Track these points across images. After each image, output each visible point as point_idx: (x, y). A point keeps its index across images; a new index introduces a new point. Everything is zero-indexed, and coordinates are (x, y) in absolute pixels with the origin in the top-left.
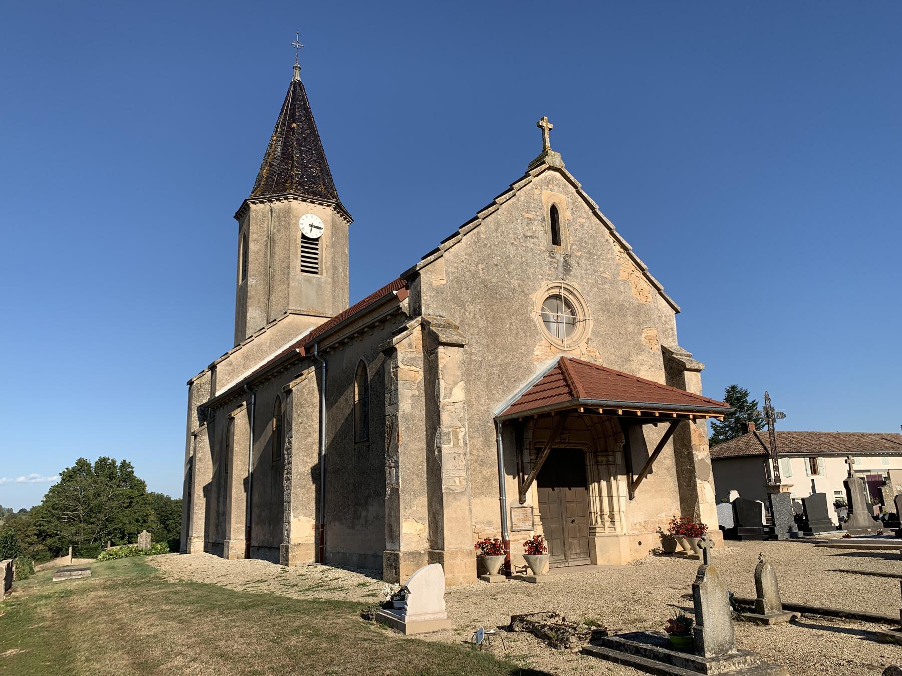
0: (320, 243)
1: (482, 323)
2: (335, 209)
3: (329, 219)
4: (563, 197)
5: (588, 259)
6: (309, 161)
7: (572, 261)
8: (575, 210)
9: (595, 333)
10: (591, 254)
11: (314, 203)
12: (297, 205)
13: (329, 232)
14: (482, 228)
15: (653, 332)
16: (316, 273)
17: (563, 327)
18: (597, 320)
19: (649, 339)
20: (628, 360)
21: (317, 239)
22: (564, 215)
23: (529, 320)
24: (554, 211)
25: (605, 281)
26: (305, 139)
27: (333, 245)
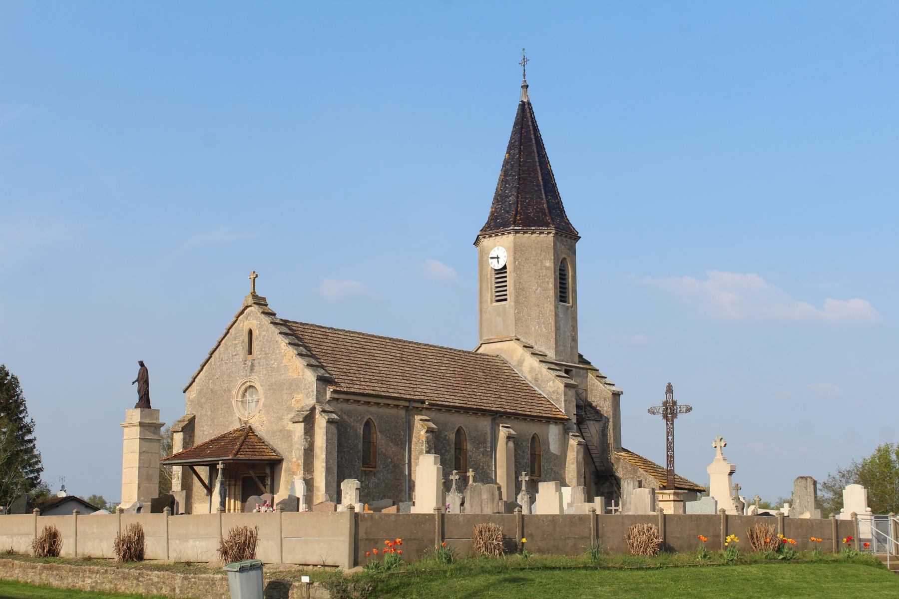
0: (508, 270)
1: (209, 413)
2: (517, 232)
3: (511, 245)
4: (255, 322)
5: (265, 358)
6: (510, 192)
7: (256, 363)
8: (261, 327)
9: (264, 406)
10: (266, 354)
11: (497, 235)
12: (486, 242)
13: (512, 258)
14: (212, 359)
15: (300, 396)
16: (506, 300)
17: (254, 404)
18: (265, 397)
19: (297, 401)
20: (281, 419)
21: (505, 267)
22: (255, 334)
23: (231, 406)
24: (250, 332)
25: (273, 369)
26: (512, 166)
27: (516, 269)
